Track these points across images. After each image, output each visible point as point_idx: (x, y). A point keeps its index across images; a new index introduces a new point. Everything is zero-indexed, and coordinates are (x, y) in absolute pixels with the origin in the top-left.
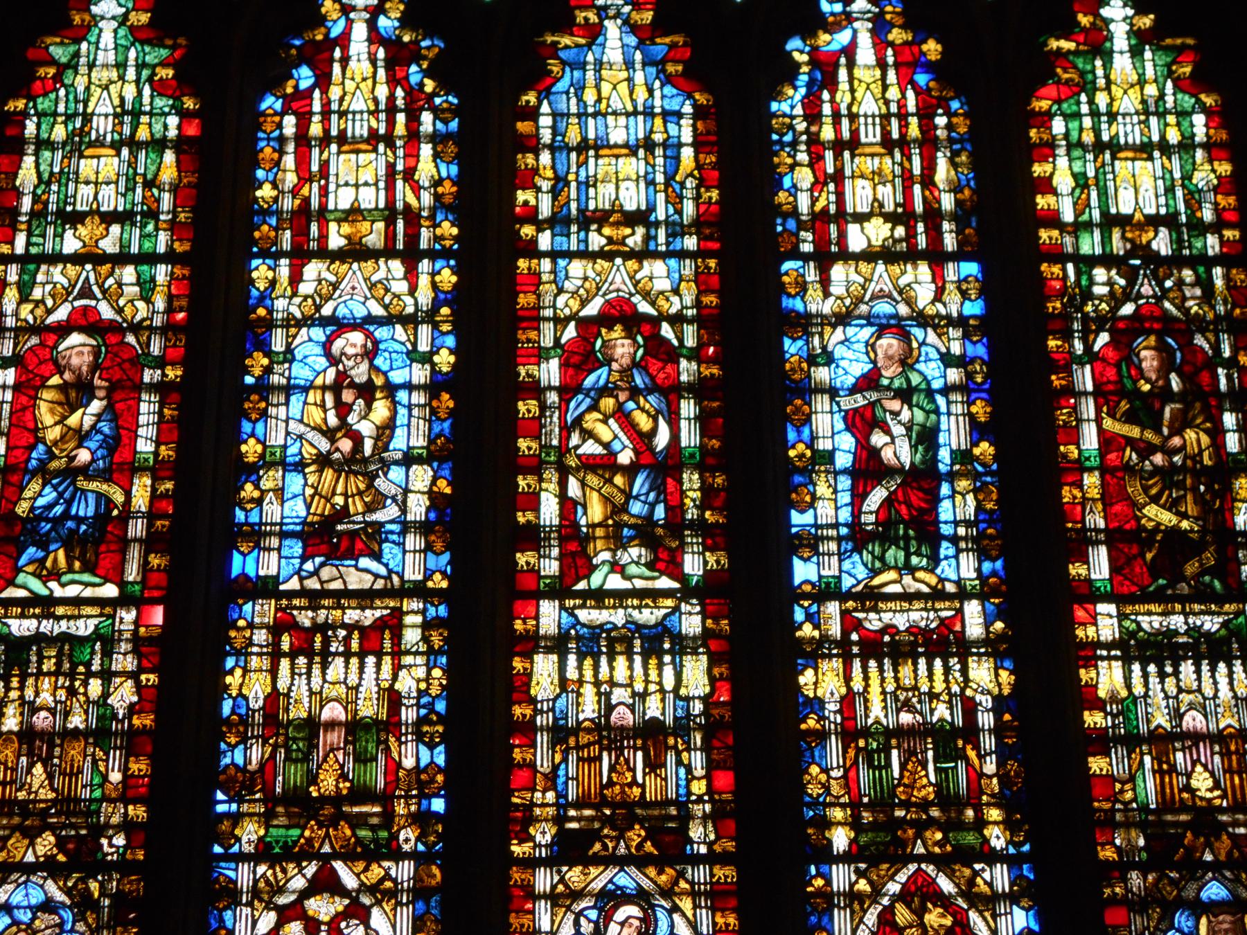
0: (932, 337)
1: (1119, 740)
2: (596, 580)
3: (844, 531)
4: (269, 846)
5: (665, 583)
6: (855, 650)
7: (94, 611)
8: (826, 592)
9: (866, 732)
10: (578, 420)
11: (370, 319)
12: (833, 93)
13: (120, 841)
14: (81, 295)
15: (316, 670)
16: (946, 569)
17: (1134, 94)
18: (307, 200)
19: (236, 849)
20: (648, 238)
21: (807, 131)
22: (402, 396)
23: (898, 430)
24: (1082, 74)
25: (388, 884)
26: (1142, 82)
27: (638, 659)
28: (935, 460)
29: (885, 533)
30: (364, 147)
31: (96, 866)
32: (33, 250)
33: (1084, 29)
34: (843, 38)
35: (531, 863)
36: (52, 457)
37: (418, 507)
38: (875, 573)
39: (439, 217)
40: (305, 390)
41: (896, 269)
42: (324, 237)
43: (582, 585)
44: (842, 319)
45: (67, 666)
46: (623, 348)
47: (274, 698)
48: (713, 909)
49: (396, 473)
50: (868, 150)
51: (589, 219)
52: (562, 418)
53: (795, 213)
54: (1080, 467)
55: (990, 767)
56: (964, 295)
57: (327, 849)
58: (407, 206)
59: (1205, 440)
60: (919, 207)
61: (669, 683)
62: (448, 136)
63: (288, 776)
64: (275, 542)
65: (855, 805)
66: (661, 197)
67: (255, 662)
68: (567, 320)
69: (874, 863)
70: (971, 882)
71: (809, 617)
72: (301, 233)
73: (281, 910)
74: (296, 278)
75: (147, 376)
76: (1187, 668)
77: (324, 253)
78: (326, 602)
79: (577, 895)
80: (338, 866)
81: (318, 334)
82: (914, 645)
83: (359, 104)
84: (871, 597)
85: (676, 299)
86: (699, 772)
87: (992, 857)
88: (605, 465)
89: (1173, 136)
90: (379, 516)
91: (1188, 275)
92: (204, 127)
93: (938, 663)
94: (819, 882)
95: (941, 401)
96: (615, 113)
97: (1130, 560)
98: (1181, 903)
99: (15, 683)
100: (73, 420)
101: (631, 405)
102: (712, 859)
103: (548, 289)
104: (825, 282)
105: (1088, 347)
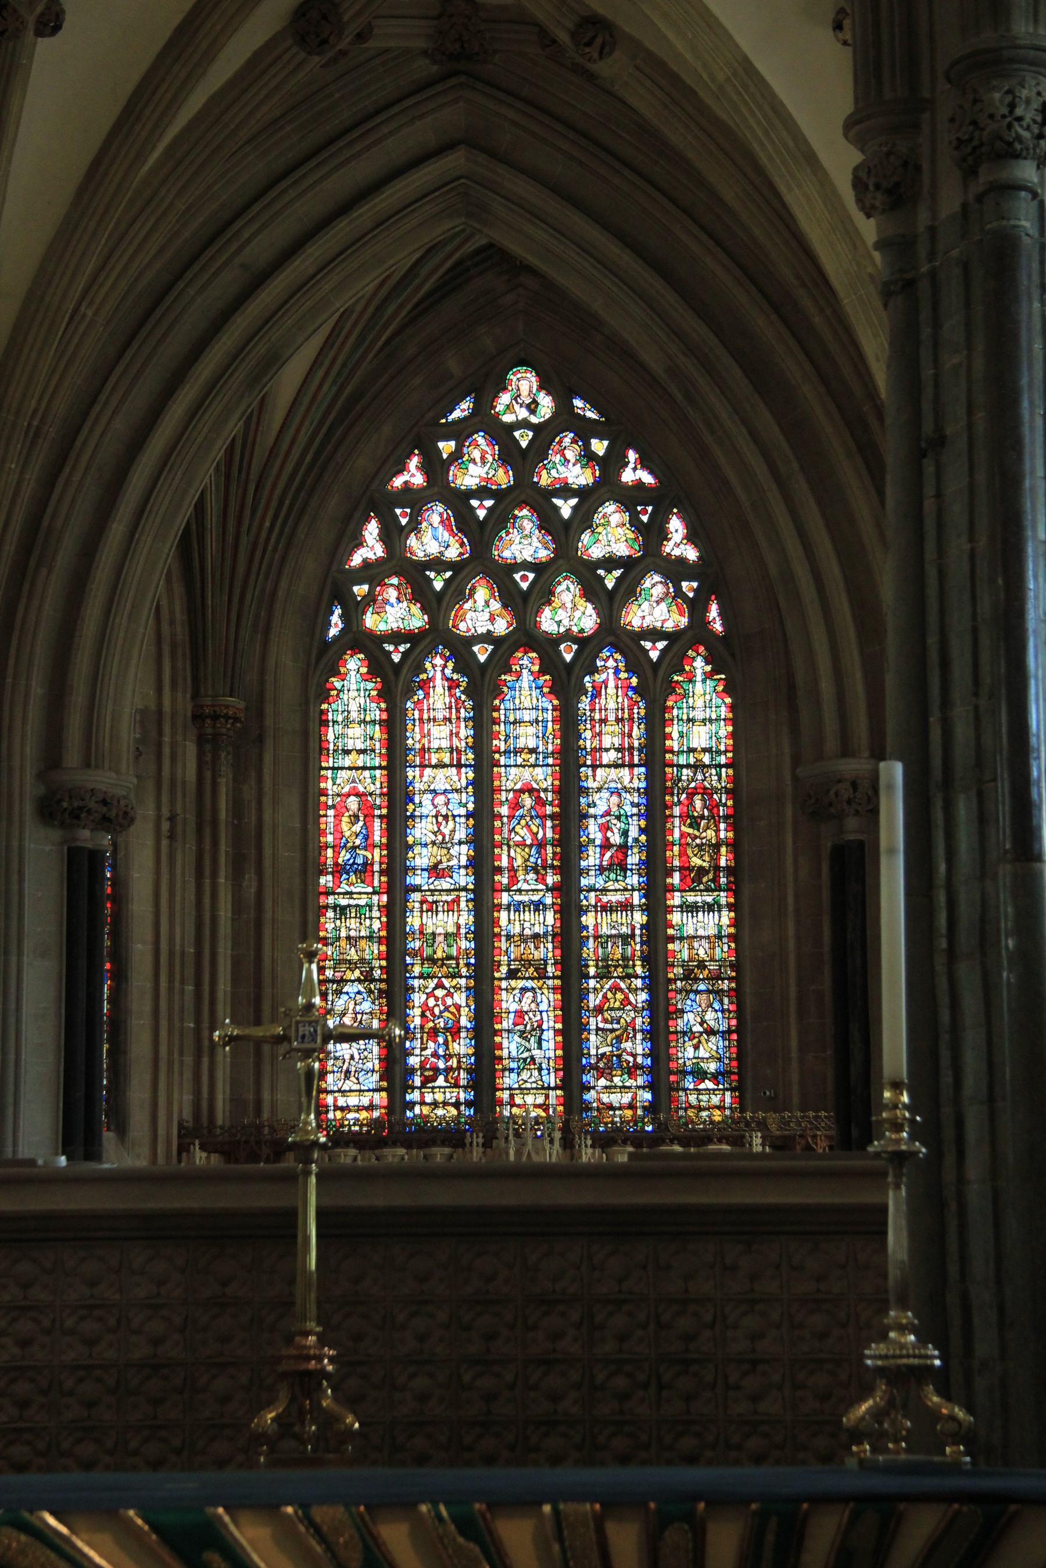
0: (628, 796)
1: (678, 938)
2: (519, 885)
3: (597, 867)
4: (423, 974)
5: (541, 887)
6: (599, 909)
7: (366, 896)
8: (591, 889)
9: (601, 937)
10: (514, 828)
11: (445, 791)
12: (600, 699)
13: (379, 972)
14: (352, 782)
15: (434, 916)
16: (628, 880)
17: (702, 699)
18: (424, 745)
19: (413, 975)
20: (537, 759)
21: (590, 716)
22: (457, 819)
23: (616, 831)
24: (685, 690)
25: (458, 986)
26: (705, 694)
27: (532, 912)
28: (627, 842)
29: (610, 868)
30: (442, 723)
31: (373, 980)
32: (336, 765)
33: (687, 672)
34: (604, 676)
35: (500, 979)
36: (348, 842)
37: (464, 861)
38: (606, 882)
39: (468, 751)
40: (427, 817)
41: (618, 770)
42: (430, 759)
43: (515, 888)
44: (599, 790)
45: (358, 915)
46: (527, 801)
47: (422, 925)
48: (554, 993)
49: (457, 847)
50: (610, 723)
51: (517, 752)
52: (509, 828)
53: (585, 748)
54: (673, 844)
55: (638, 947)
56: (639, 779)
57: (440, 975)
58: (457, 747)
59: (714, 834)
60: (627, 746)
61: (542, 921)
62: (470, 718)
63: (428, 951)
64: (419, 872)
65: (597, 960)
66: (541, 742)
67: (415, 914)
68: (510, 790)
69: (602, 979)
70: (630, 985)
71: (585, 898)
72: (423, 757)
73: (427, 994)
74: (421, 776)
75: (377, 812)
76: (700, 914)
77: (430, 766)
78: (436, 893)
79: (513, 989)
80: (443, 980)
81: (430, 796)
82: (617, 907)
83: (439, 705)
84: (605, 891)
85: (545, 782)
86: (550, 949)
87: (636, 977)
88: (522, 844)
89: (714, 717)
90: (451, 864)
91: (713, 771)
92: (388, 715)
93: (624, 913)
94: (585, 985)
95: (630, 819)
96: (526, 709)
97: (686, 876)
98: (691, 991)
99: (343, 920)
100: (354, 829)
101: (530, 823)
102: (554, 978)
103: (504, 779)
104: (594, 776)
105: (679, 800)
